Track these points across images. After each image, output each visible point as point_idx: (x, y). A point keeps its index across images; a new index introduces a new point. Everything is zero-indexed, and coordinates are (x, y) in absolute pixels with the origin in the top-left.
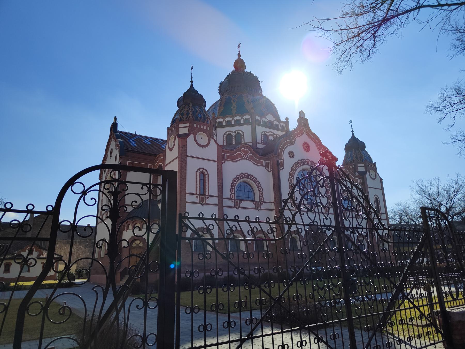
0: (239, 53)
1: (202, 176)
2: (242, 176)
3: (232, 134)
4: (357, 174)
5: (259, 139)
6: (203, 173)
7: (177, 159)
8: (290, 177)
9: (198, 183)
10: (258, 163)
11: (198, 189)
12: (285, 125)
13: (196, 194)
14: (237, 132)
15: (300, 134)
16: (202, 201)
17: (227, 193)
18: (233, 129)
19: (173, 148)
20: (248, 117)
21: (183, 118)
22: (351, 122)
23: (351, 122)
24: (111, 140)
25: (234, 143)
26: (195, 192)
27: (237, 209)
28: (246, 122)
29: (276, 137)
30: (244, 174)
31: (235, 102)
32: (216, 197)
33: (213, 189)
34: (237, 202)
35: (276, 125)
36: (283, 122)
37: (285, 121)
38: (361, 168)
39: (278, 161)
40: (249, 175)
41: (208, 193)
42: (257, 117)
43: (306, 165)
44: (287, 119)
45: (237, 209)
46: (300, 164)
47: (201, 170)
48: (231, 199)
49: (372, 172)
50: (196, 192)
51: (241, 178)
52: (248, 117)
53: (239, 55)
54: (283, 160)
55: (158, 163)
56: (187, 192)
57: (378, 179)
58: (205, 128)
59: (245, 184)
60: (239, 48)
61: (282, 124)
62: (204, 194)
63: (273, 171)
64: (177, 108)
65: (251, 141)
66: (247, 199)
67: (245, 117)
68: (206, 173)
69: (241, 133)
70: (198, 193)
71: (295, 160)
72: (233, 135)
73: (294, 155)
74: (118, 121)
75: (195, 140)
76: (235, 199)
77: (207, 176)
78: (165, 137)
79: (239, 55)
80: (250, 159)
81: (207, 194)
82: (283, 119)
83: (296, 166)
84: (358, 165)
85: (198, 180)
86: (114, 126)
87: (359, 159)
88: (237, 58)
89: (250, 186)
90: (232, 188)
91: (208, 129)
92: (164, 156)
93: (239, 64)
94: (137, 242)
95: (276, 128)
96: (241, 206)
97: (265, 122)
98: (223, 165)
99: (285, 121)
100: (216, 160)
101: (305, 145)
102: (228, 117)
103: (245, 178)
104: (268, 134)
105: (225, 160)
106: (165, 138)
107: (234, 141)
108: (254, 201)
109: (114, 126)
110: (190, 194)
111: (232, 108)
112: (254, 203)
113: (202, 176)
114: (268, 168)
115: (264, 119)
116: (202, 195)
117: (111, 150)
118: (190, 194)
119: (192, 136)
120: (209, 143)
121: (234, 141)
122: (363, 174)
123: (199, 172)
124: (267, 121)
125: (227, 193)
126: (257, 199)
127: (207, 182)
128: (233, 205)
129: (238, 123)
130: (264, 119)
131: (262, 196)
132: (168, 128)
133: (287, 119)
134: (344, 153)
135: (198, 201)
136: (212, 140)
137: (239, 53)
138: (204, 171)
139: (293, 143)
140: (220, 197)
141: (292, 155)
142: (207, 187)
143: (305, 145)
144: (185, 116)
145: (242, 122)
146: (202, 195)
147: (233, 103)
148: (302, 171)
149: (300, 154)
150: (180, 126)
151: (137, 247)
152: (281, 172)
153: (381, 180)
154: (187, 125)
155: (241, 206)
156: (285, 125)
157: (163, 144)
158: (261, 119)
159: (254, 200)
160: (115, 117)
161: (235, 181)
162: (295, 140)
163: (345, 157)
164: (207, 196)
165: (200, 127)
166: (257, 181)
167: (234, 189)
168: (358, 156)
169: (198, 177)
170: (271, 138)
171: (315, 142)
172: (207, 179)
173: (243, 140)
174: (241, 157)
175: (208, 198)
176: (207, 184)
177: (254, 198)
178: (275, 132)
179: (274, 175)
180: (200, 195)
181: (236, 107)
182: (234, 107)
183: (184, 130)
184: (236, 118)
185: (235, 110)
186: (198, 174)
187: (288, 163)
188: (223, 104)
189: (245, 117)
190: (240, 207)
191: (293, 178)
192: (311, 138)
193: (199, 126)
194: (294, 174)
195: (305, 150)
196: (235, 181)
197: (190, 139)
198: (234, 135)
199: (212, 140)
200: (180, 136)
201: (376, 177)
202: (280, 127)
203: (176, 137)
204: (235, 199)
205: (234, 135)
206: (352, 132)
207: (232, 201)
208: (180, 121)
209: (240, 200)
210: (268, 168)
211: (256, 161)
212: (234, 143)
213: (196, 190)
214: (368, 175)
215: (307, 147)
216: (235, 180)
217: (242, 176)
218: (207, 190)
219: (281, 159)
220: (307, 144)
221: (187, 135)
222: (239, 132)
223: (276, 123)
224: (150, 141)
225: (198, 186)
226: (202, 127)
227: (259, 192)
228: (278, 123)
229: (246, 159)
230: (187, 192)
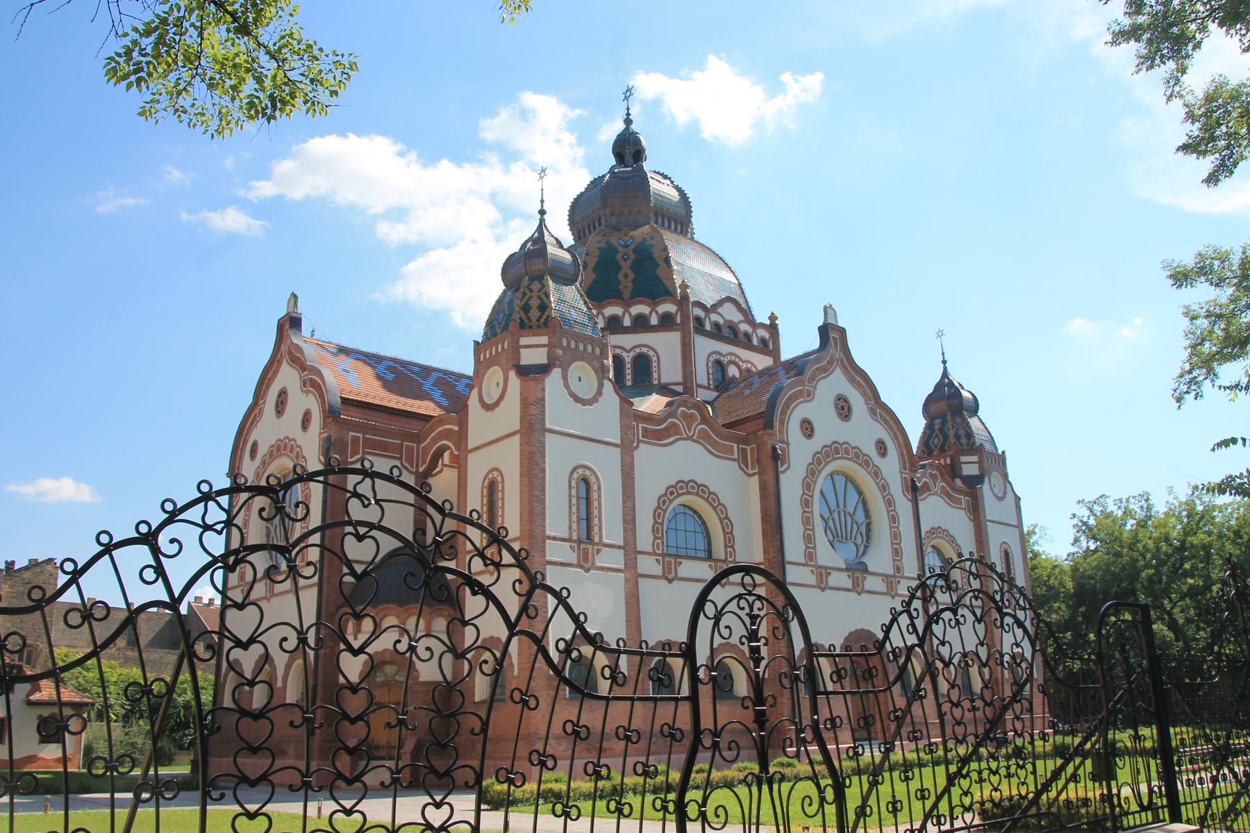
0: (628, 114)
1: (585, 488)
2: (681, 488)
3: (625, 354)
4: (958, 482)
5: (702, 374)
6: (585, 480)
7: (517, 437)
8: (804, 493)
9: (574, 509)
10: (719, 451)
11: (574, 526)
12: (767, 335)
13: (569, 540)
14: (637, 350)
15: (825, 371)
16: (586, 559)
17: (645, 539)
18: (627, 342)
19: (497, 404)
20: (670, 308)
21: (528, 318)
22: (940, 334)
23: (940, 334)
24: (280, 363)
25: (629, 383)
26: (566, 536)
27: (670, 581)
28: (667, 322)
29: (748, 370)
30: (687, 484)
31: (629, 262)
32: (619, 547)
33: (610, 528)
34: (669, 563)
35: (747, 335)
36: (762, 325)
37: (768, 322)
38: (970, 469)
39: (774, 449)
40: (699, 486)
41: (601, 537)
42: (698, 312)
43: (843, 458)
44: (773, 318)
45: (670, 581)
46: (828, 456)
47: (581, 471)
48: (654, 554)
49: (995, 478)
50: (571, 534)
51: (679, 495)
52: (672, 308)
53: (628, 121)
54: (788, 444)
55: (435, 440)
56: (548, 533)
57: (1010, 498)
58: (589, 349)
59: (688, 511)
60: (626, 98)
61: (762, 333)
62: (589, 537)
63: (760, 474)
64: (497, 287)
65: (680, 379)
66: (692, 553)
67: (662, 309)
68: (593, 479)
69: (651, 353)
70: (575, 537)
71: (816, 443)
72: (628, 358)
73: (812, 430)
74: (302, 308)
75: (567, 386)
76: (663, 555)
77: (595, 487)
78: (468, 368)
79: (628, 121)
80: (703, 439)
81: (596, 539)
82: (762, 317)
83: (819, 463)
84: (963, 459)
85: (574, 501)
86: (291, 322)
87: (964, 441)
88: (621, 126)
89: (700, 517)
90: (656, 522)
91: (598, 351)
92: (463, 423)
93: (628, 149)
94: (390, 670)
95: (744, 341)
96: (680, 574)
97: (716, 325)
98: (636, 454)
99: (768, 322)
100: (618, 442)
101: (841, 403)
102: (610, 304)
103: (688, 493)
104: (725, 360)
105: (639, 441)
106: (469, 371)
107: (629, 377)
108: (709, 557)
109: (291, 322)
110: (555, 539)
111: (621, 277)
112: (710, 566)
113: (585, 488)
114: (747, 466)
115: (714, 317)
116: (586, 538)
117: (283, 395)
118: (555, 539)
119: (556, 372)
120: (599, 393)
121: (629, 377)
122: (973, 484)
123: (575, 476)
124: (721, 321)
125: (645, 539)
126: (719, 550)
127: (596, 504)
128: (657, 570)
129: (640, 324)
130: (714, 317)
131: (732, 547)
132: (476, 343)
133: (773, 318)
134: (922, 422)
135: (575, 562)
136: (606, 382)
137: (628, 114)
138: (588, 473)
139: (810, 395)
140: (630, 549)
141: (808, 429)
142: (596, 521)
143: (841, 403)
144: (534, 314)
145: (654, 321)
146: (586, 538)
147: (622, 263)
148: (831, 475)
149: (829, 429)
150: (524, 341)
151: (389, 684)
152: (782, 477)
153: (1018, 499)
154: (544, 340)
155: (680, 574)
156: (767, 335)
157: (426, 378)
158: (707, 315)
159: (709, 557)
160: (294, 296)
161: (664, 502)
162: (815, 388)
163: (924, 433)
164: (598, 544)
165: (577, 346)
166: (720, 504)
167: (662, 524)
168: (961, 432)
169: (574, 492)
170: (733, 371)
171: (864, 395)
172: (595, 496)
173: (655, 375)
174: (679, 433)
175: (598, 551)
176: (596, 512)
177: (710, 552)
178: (745, 354)
179: (763, 487)
180: (579, 542)
181: (632, 276)
182: (626, 276)
183: (533, 355)
184: (639, 309)
185: (630, 286)
186: (574, 484)
187: (800, 451)
188: (591, 265)
189: (662, 309)
190: (676, 578)
191: (812, 497)
192: (852, 381)
193: (573, 345)
194: (815, 483)
195: (840, 415)
196: (664, 502)
197: (553, 380)
198: (628, 360)
199: (606, 382)
200: (525, 372)
201: (1005, 493)
202: (755, 342)
203: (512, 374)
204: (663, 555)
205: (628, 360)
206: (944, 362)
207: (658, 561)
208: (522, 325)
209: (677, 556)
210: (747, 466)
211: (715, 445)
212: (629, 383)
213: (570, 528)
214: (986, 487)
215: (843, 409)
216: (663, 501)
217: (681, 488)
218: (596, 529)
219: (782, 441)
220: (846, 401)
221: (544, 370)
222: (644, 350)
223: (744, 327)
224: (389, 368)
225: (574, 518)
226: (581, 348)
227: (725, 533)
228: (749, 329)
229: (690, 438)
230: (548, 533)
